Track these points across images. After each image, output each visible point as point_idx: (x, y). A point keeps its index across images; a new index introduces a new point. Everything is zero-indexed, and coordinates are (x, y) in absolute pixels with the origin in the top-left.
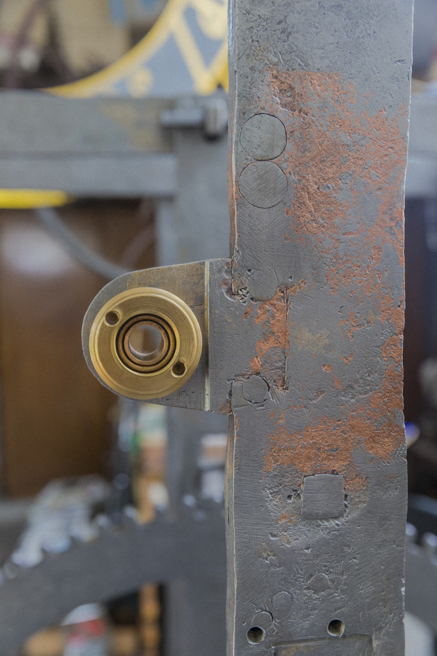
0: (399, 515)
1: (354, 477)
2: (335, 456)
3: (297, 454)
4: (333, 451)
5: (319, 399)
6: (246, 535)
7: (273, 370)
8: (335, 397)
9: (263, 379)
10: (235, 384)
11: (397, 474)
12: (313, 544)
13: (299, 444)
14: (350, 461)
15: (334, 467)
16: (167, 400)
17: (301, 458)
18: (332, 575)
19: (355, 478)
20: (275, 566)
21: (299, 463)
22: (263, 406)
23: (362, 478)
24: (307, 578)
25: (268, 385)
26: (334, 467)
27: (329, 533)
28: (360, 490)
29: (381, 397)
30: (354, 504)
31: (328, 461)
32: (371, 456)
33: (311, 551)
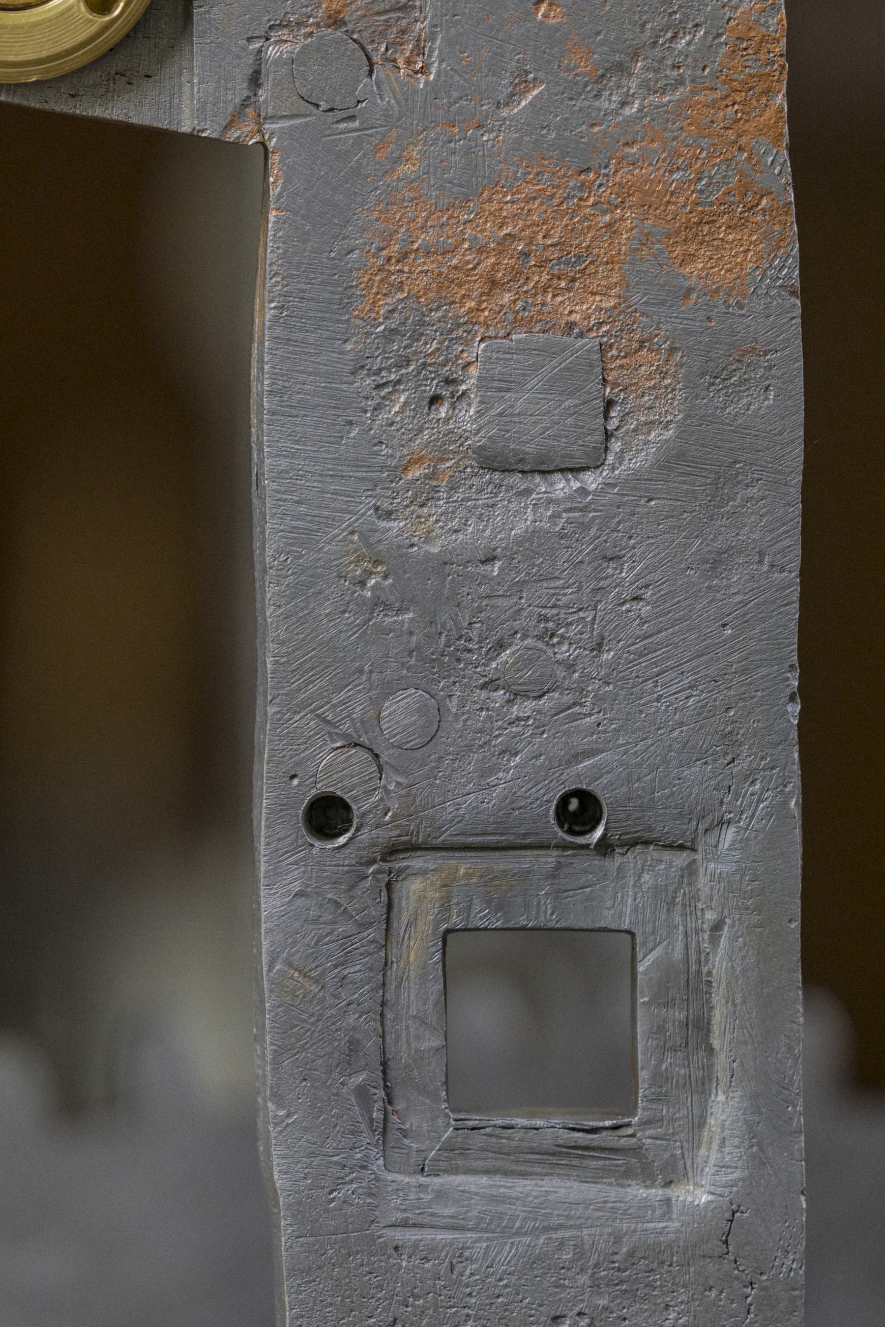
0: (777, 472)
1: (635, 345)
2: (573, 280)
3: (456, 268)
4: (567, 263)
5: (523, 103)
6: (302, 509)
7: (386, 12)
8: (571, 99)
9: (355, 41)
10: (272, 52)
11: (769, 343)
12: (505, 549)
13: (464, 240)
14: (619, 297)
15: (571, 312)
16: (73, 96)
17: (469, 282)
18: (565, 648)
19: (636, 352)
20: (388, 607)
21: (463, 296)
22: (352, 118)
23: (658, 350)
24: (487, 653)
25: (369, 59)
26: (571, 312)
27: (555, 516)
28: (654, 387)
29: (715, 101)
30: (634, 431)
31: (554, 296)
32: (687, 284)
33: (501, 569)
